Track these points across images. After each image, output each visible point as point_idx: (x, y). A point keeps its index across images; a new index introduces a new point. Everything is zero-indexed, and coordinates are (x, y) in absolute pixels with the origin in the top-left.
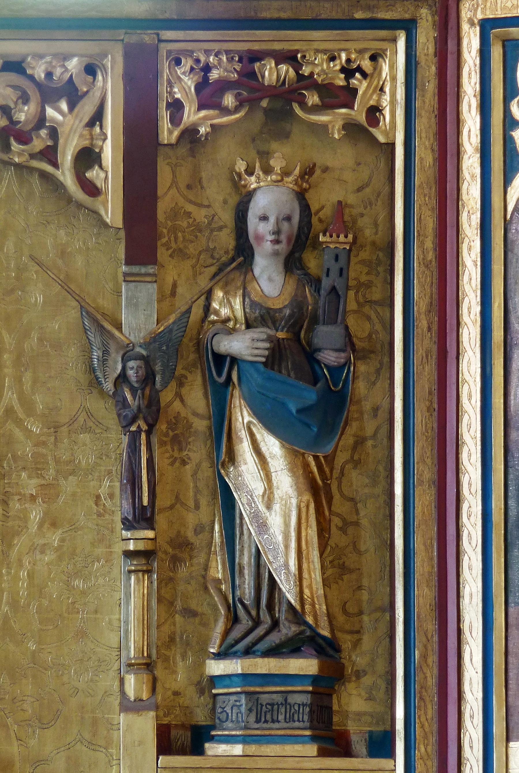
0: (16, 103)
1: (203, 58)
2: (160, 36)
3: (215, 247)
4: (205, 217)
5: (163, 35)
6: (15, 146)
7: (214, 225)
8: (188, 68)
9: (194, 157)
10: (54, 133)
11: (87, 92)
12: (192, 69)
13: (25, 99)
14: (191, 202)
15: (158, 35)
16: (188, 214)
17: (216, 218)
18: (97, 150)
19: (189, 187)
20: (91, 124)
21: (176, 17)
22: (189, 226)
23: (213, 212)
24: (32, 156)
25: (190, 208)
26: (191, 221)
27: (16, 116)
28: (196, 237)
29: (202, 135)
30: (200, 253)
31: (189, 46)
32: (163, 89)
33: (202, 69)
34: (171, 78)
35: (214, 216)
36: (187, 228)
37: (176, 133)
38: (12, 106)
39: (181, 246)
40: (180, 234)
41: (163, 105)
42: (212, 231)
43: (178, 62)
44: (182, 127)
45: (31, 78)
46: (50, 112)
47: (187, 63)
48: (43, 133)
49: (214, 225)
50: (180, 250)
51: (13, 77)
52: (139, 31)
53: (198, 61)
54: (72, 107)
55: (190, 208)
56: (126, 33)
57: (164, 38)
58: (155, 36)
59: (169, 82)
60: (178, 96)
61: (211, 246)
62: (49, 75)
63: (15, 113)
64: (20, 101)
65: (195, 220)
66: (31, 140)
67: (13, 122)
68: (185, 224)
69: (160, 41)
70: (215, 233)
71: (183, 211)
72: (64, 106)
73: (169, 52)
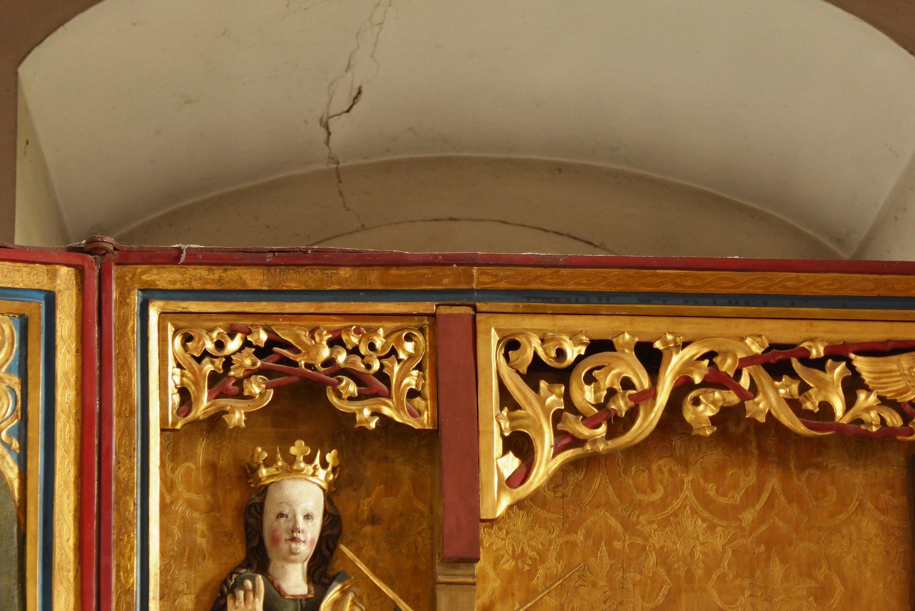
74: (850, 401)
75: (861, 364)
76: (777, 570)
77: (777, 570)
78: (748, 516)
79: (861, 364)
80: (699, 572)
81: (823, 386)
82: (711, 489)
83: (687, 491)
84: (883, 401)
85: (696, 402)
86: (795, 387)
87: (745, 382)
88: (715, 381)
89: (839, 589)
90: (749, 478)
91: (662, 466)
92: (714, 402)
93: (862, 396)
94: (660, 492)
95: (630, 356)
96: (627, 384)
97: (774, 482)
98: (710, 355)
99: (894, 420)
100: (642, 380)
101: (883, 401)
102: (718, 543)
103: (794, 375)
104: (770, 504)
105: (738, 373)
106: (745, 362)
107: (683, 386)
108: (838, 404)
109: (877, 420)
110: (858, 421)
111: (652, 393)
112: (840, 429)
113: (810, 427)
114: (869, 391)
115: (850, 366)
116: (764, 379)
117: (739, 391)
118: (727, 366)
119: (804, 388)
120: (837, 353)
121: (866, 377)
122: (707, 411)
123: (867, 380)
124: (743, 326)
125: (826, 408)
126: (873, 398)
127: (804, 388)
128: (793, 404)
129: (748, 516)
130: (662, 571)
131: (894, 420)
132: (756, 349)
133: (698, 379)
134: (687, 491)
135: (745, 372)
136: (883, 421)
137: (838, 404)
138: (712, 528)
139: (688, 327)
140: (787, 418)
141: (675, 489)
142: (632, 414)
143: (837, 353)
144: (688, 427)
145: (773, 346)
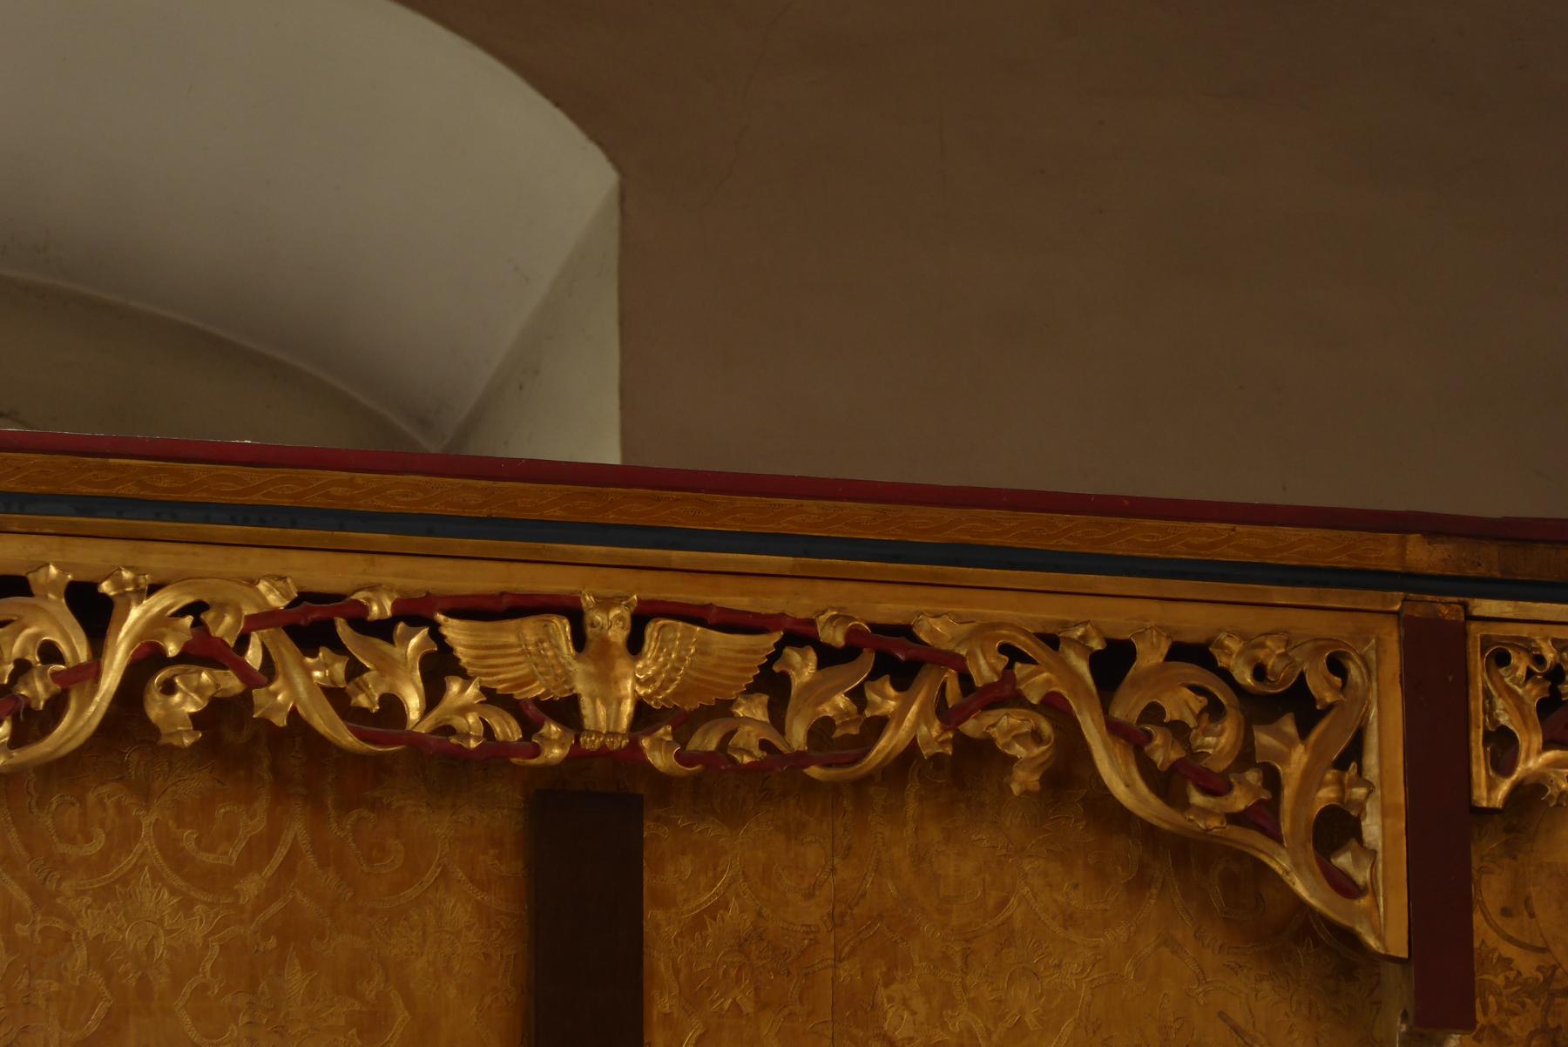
0: (1198, 717)
1: (1550, 656)
2: (1470, 608)
3: (1559, 1027)
4: (1539, 969)
5: (1475, 607)
6: (1197, 798)
7: (1556, 986)
8: (1521, 672)
9: (1515, 858)
10: (1272, 780)
11: (1330, 707)
12: (1530, 673)
13: (1215, 710)
14: (1510, 940)
15: (1465, 606)
16: (1507, 963)
17: (1559, 972)
18: (1353, 813)
19: (1506, 912)
20: (1341, 764)
21: (1498, 575)
22: (1509, 983)
23: (1553, 962)
24: (1234, 819)
25: (1508, 950)
26: (1512, 975)
27: (1199, 742)
28: (1523, 1005)
29: (1551, 797)
30: (1532, 1035)
31: (1525, 631)
32: (1477, 705)
33: (1547, 676)
34: (1491, 688)
35: (1554, 968)
36: (1505, 987)
37: (1505, 787)
38: (1191, 722)
39: (1495, 1021)
40: (1491, 999)
41: (1477, 736)
42: (1553, 995)
43: (1502, 659)
44: (1514, 777)
45: (1225, 675)
46: (1264, 739)
47: (1521, 664)
48: (1252, 776)
49: (1556, 986)
50: (1493, 1027)
51: (1193, 672)
52: (1429, 598)
53: (1539, 660)
54: (1304, 731)
55: (1508, 950)
56: (1404, 600)
57: (1476, 612)
58: (1459, 607)
59: (1487, 693)
60: (1504, 720)
61: (1552, 1023)
62: (1259, 672)
63: (1195, 739)
64: (1206, 716)
65: (1519, 974)
66: (1229, 788)
67: (1194, 755)
68: (1500, 980)
69: (1470, 618)
70: (1558, 1000)
71: (1496, 955)
72: (1289, 726)
73: (1486, 642)
74: (433, 696)
75: (455, 631)
76: (296, 980)
77: (296, 980)
78: (251, 887)
79: (455, 631)
80: (161, 982)
81: (388, 667)
82: (188, 839)
83: (146, 841)
84: (491, 697)
85: (169, 688)
86: (339, 668)
87: (253, 656)
88: (203, 652)
89: (402, 1015)
90: (255, 822)
91: (105, 796)
92: (199, 690)
93: (455, 687)
94: (99, 842)
95: (57, 604)
96: (50, 653)
97: (296, 830)
98: (197, 609)
99: (507, 729)
100: (77, 648)
101: (491, 697)
102: (198, 931)
103: (338, 648)
104: (289, 866)
105: (243, 642)
106: (256, 622)
107: (147, 660)
108: (414, 702)
109: (479, 730)
110: (446, 730)
111: (93, 671)
112: (415, 742)
113: (362, 737)
114: (467, 678)
115: (436, 634)
116: (287, 651)
117: (243, 670)
118: (224, 627)
119: (354, 670)
120: (414, 612)
121: (463, 654)
122: (187, 704)
123: (464, 660)
124: (254, 560)
125: (392, 705)
126: (472, 691)
127: (354, 670)
128: (336, 697)
129: (251, 887)
130: (97, 978)
131: (507, 729)
132: (275, 600)
133: (172, 649)
134: (146, 841)
135: (255, 639)
136: (488, 730)
137: (414, 702)
138: (187, 905)
139: (159, 559)
140: (325, 720)
141: (129, 835)
142: (57, 706)
143: (414, 612)
144: (152, 730)
145: (305, 597)
